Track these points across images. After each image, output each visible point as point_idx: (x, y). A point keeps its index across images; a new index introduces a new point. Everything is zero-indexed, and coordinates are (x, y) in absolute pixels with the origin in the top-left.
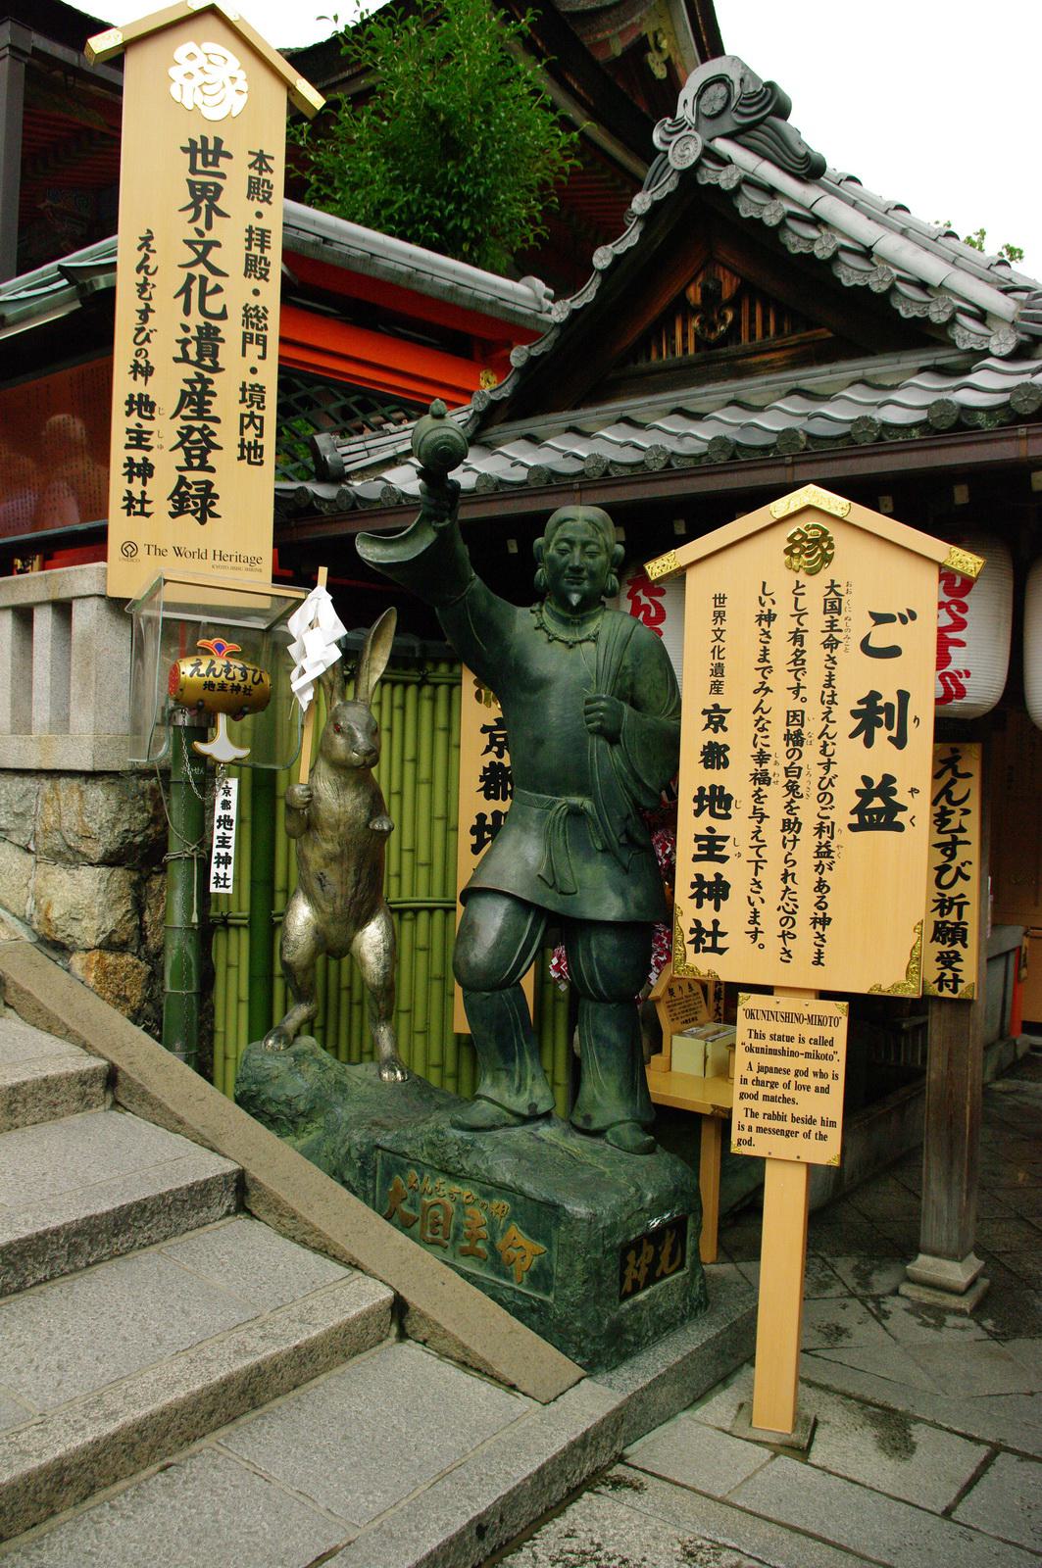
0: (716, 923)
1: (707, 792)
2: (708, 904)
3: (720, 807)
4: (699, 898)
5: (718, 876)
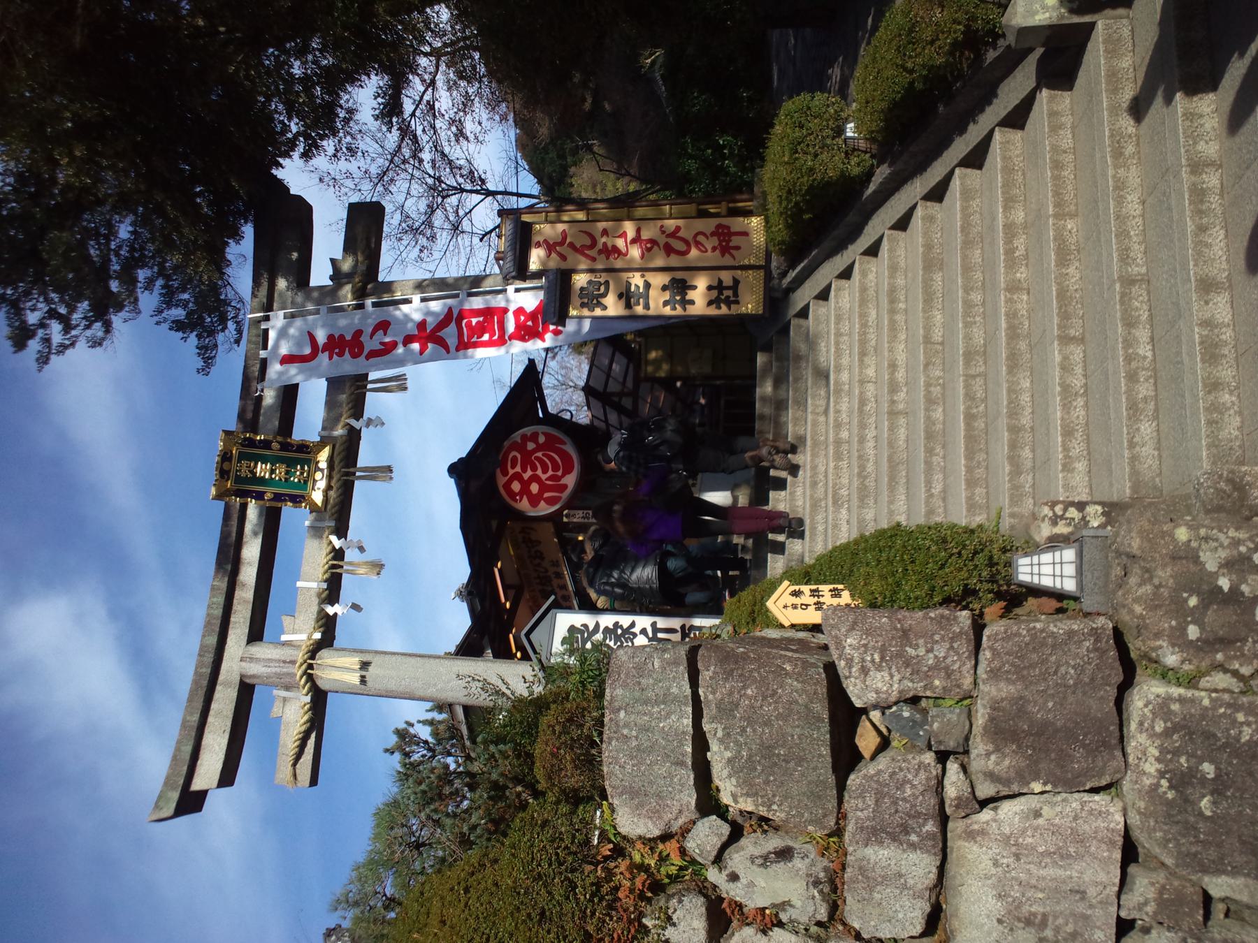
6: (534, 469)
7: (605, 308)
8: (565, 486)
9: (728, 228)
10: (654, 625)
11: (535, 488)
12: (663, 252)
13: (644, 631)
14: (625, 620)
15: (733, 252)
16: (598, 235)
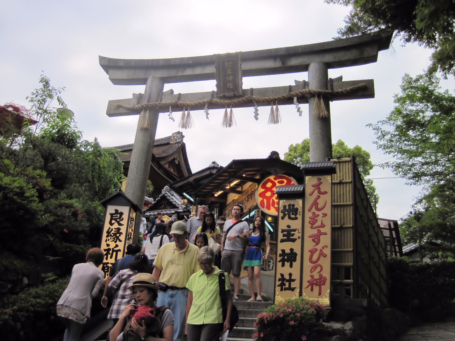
0: (290, 275)
1: (287, 208)
2: (287, 264)
3: (293, 214)
4: (283, 261)
5: (292, 250)
7: (283, 218)
8: (269, 208)
9: (324, 284)
10: (120, 250)
12: (311, 248)
13: (117, 246)
14: (122, 237)
15: (310, 287)
16: (324, 211)
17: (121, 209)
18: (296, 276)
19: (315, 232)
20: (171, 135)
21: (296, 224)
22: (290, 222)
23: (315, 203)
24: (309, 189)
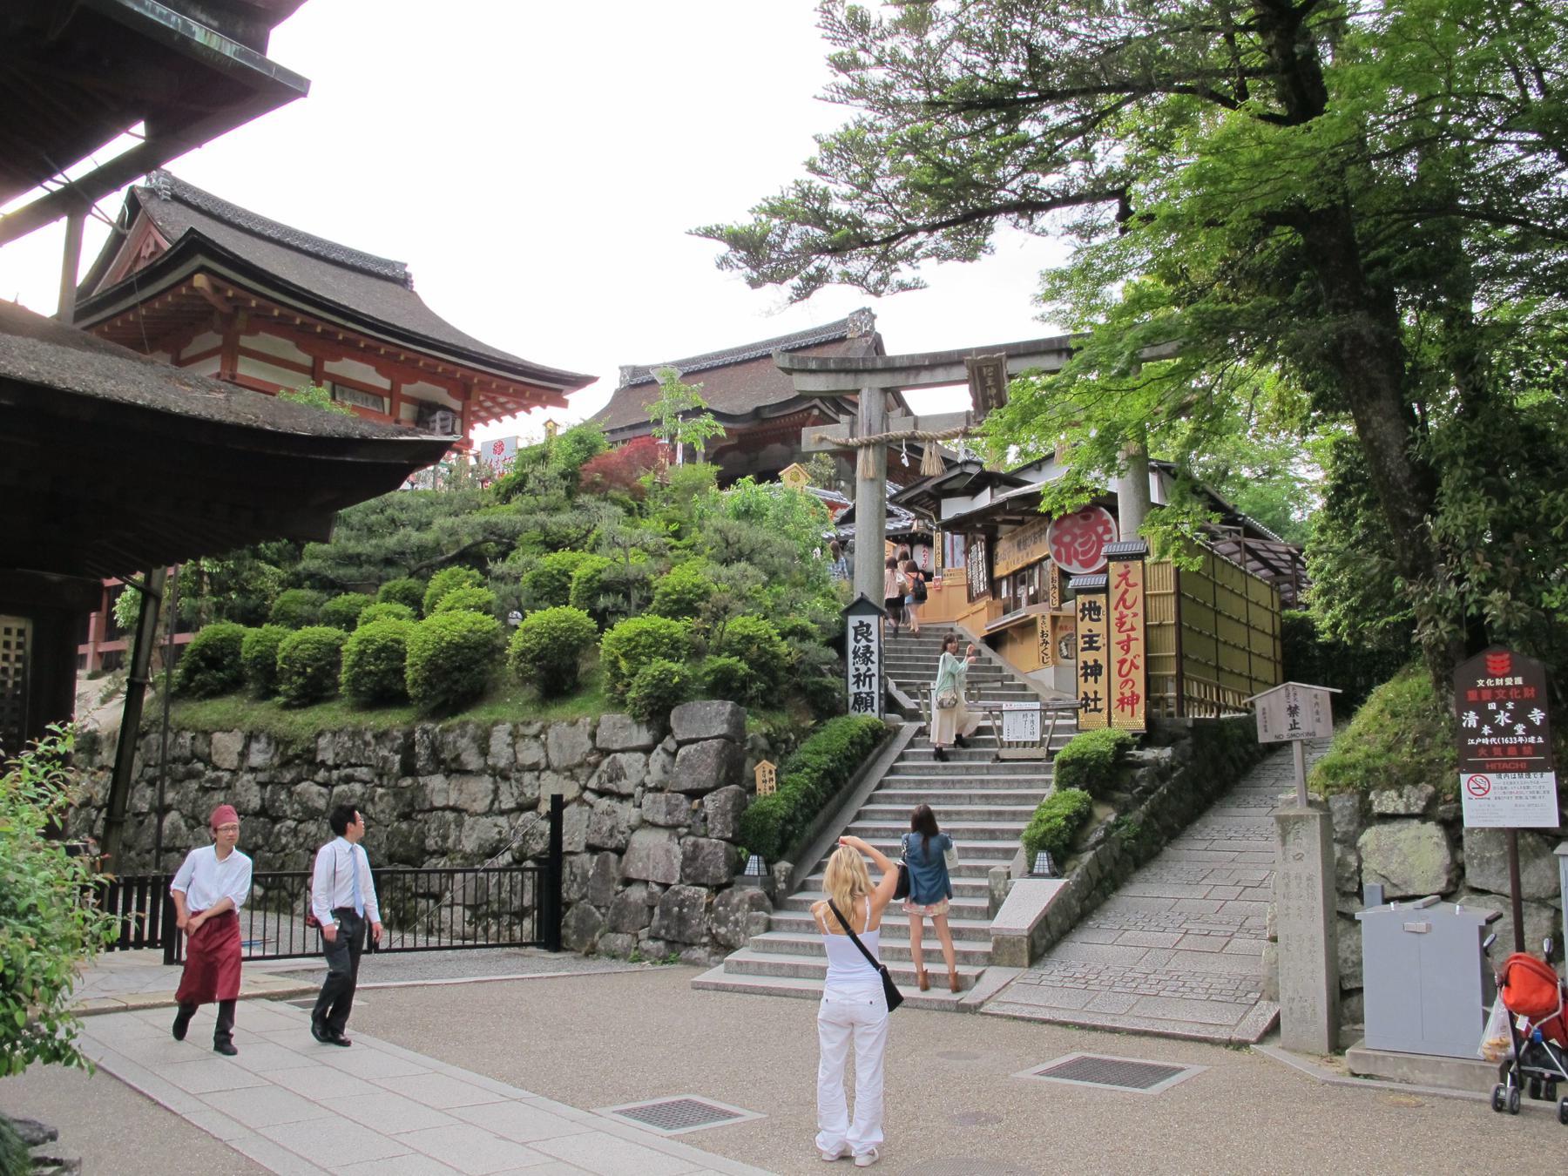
2: (1091, 679)
4: (1086, 675)
6: (1082, 535)
11: (1067, 539)
14: (875, 658)
16: (1134, 610)
17: (866, 619)
18: (1102, 694)
19: (1124, 637)
20: (846, 316)
21: (1099, 628)
22: (1092, 625)
23: (1122, 599)
24: (1114, 581)
